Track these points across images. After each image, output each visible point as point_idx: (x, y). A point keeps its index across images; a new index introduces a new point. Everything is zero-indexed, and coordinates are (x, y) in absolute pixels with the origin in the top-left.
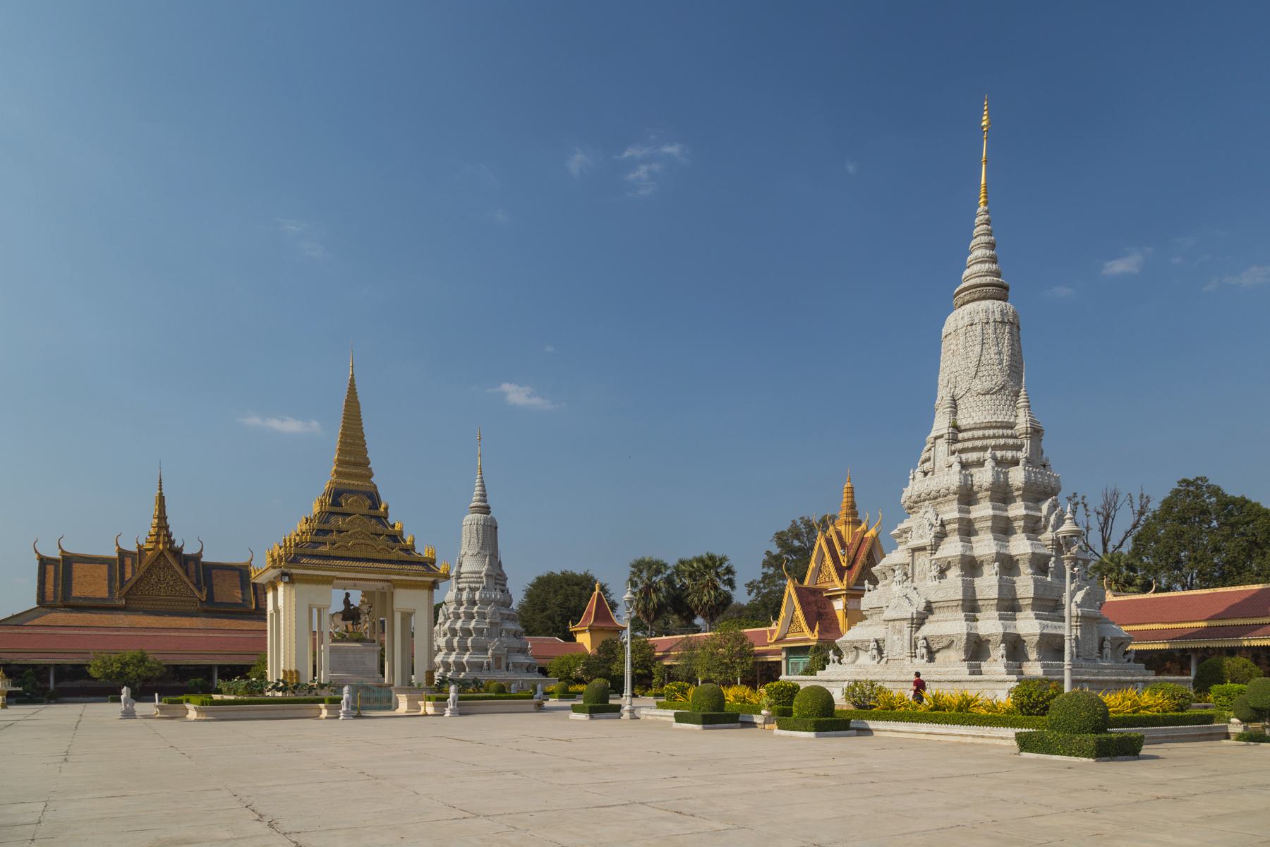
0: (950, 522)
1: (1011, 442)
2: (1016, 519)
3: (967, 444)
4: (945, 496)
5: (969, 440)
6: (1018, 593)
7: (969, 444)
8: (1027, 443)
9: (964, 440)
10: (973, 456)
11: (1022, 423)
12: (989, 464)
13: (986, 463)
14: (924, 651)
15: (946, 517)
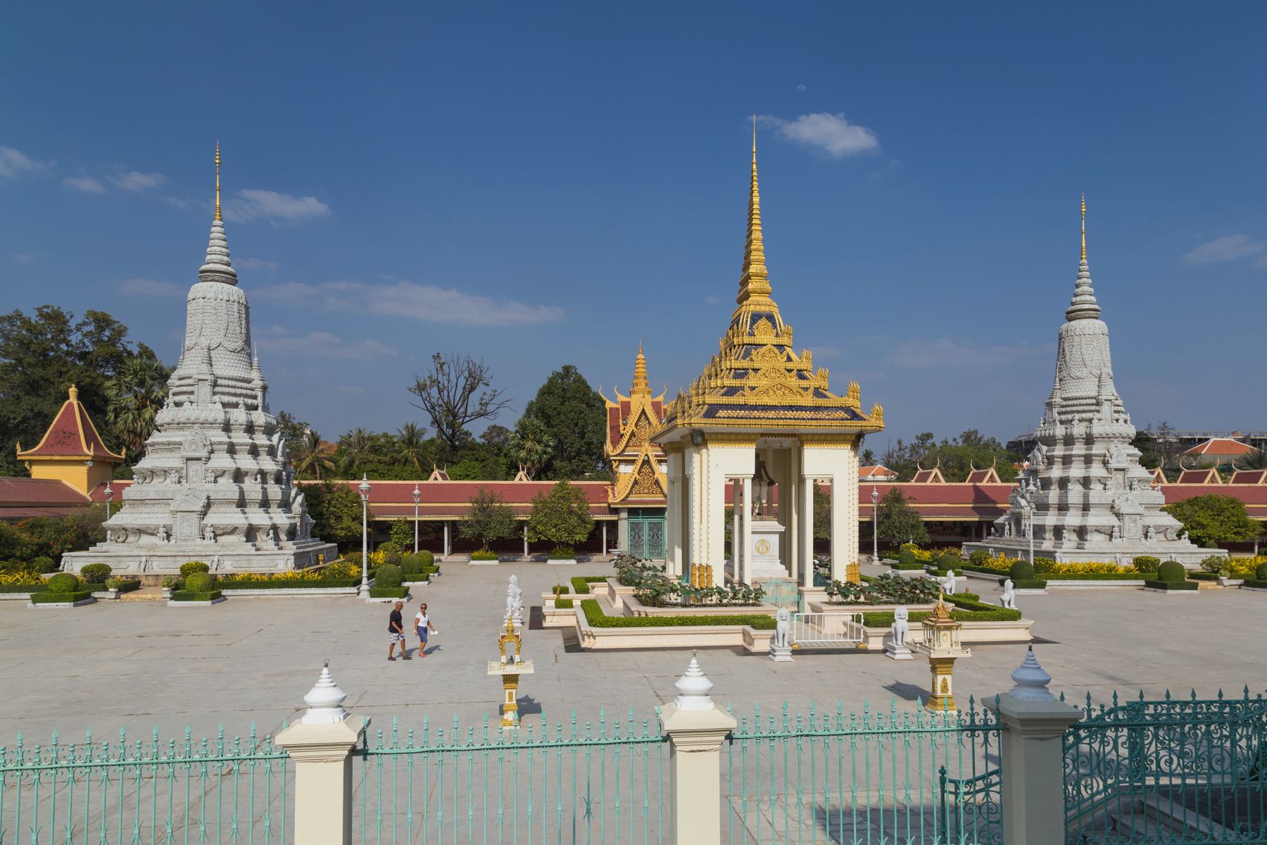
0: (221, 443)
1: (249, 392)
2: (262, 446)
3: (227, 390)
4: (211, 424)
5: (225, 386)
6: (269, 496)
7: (227, 390)
8: (259, 394)
9: (221, 386)
10: (234, 399)
11: (257, 383)
12: (242, 408)
13: (240, 406)
14: (212, 535)
15: (214, 440)
